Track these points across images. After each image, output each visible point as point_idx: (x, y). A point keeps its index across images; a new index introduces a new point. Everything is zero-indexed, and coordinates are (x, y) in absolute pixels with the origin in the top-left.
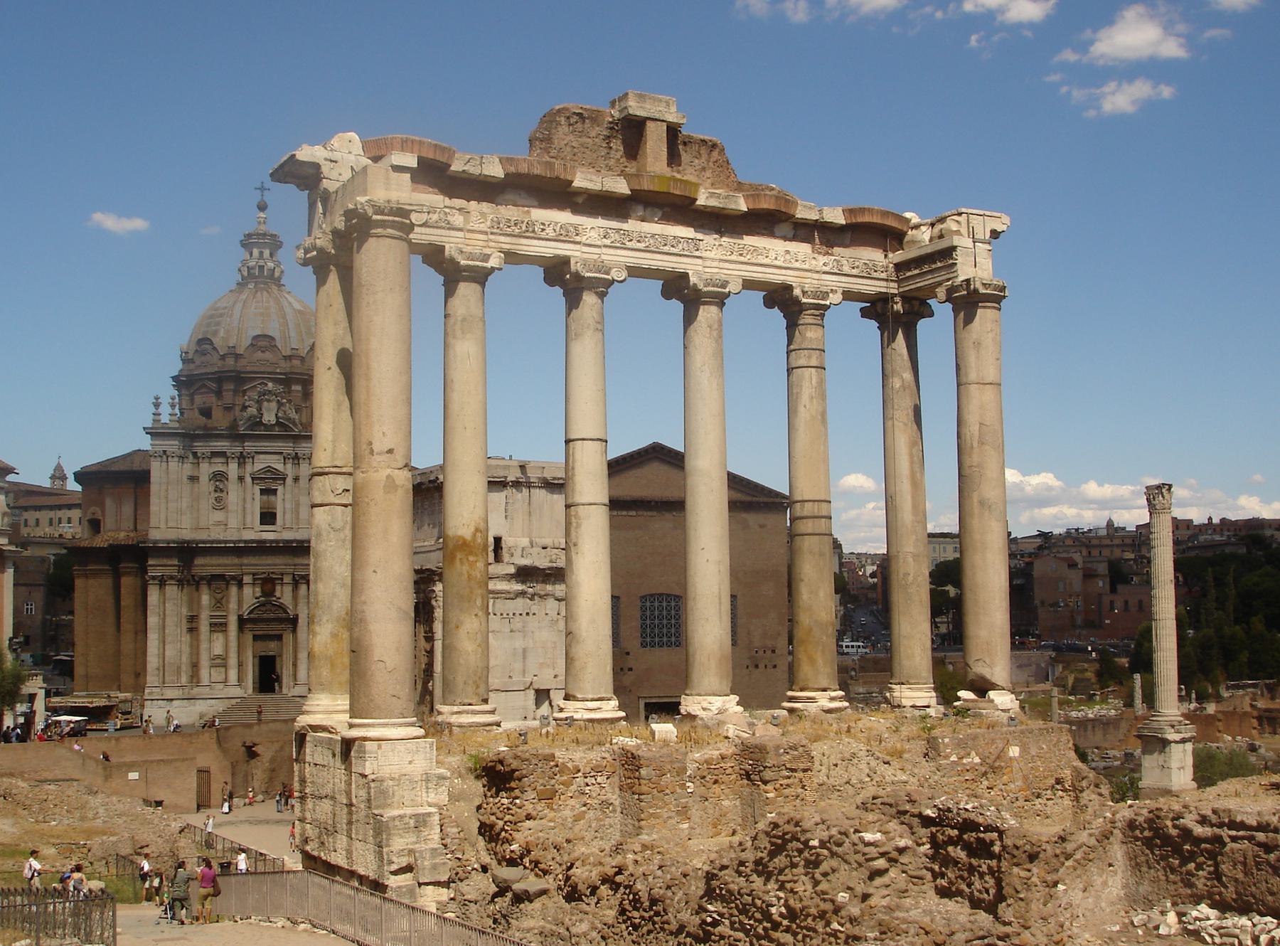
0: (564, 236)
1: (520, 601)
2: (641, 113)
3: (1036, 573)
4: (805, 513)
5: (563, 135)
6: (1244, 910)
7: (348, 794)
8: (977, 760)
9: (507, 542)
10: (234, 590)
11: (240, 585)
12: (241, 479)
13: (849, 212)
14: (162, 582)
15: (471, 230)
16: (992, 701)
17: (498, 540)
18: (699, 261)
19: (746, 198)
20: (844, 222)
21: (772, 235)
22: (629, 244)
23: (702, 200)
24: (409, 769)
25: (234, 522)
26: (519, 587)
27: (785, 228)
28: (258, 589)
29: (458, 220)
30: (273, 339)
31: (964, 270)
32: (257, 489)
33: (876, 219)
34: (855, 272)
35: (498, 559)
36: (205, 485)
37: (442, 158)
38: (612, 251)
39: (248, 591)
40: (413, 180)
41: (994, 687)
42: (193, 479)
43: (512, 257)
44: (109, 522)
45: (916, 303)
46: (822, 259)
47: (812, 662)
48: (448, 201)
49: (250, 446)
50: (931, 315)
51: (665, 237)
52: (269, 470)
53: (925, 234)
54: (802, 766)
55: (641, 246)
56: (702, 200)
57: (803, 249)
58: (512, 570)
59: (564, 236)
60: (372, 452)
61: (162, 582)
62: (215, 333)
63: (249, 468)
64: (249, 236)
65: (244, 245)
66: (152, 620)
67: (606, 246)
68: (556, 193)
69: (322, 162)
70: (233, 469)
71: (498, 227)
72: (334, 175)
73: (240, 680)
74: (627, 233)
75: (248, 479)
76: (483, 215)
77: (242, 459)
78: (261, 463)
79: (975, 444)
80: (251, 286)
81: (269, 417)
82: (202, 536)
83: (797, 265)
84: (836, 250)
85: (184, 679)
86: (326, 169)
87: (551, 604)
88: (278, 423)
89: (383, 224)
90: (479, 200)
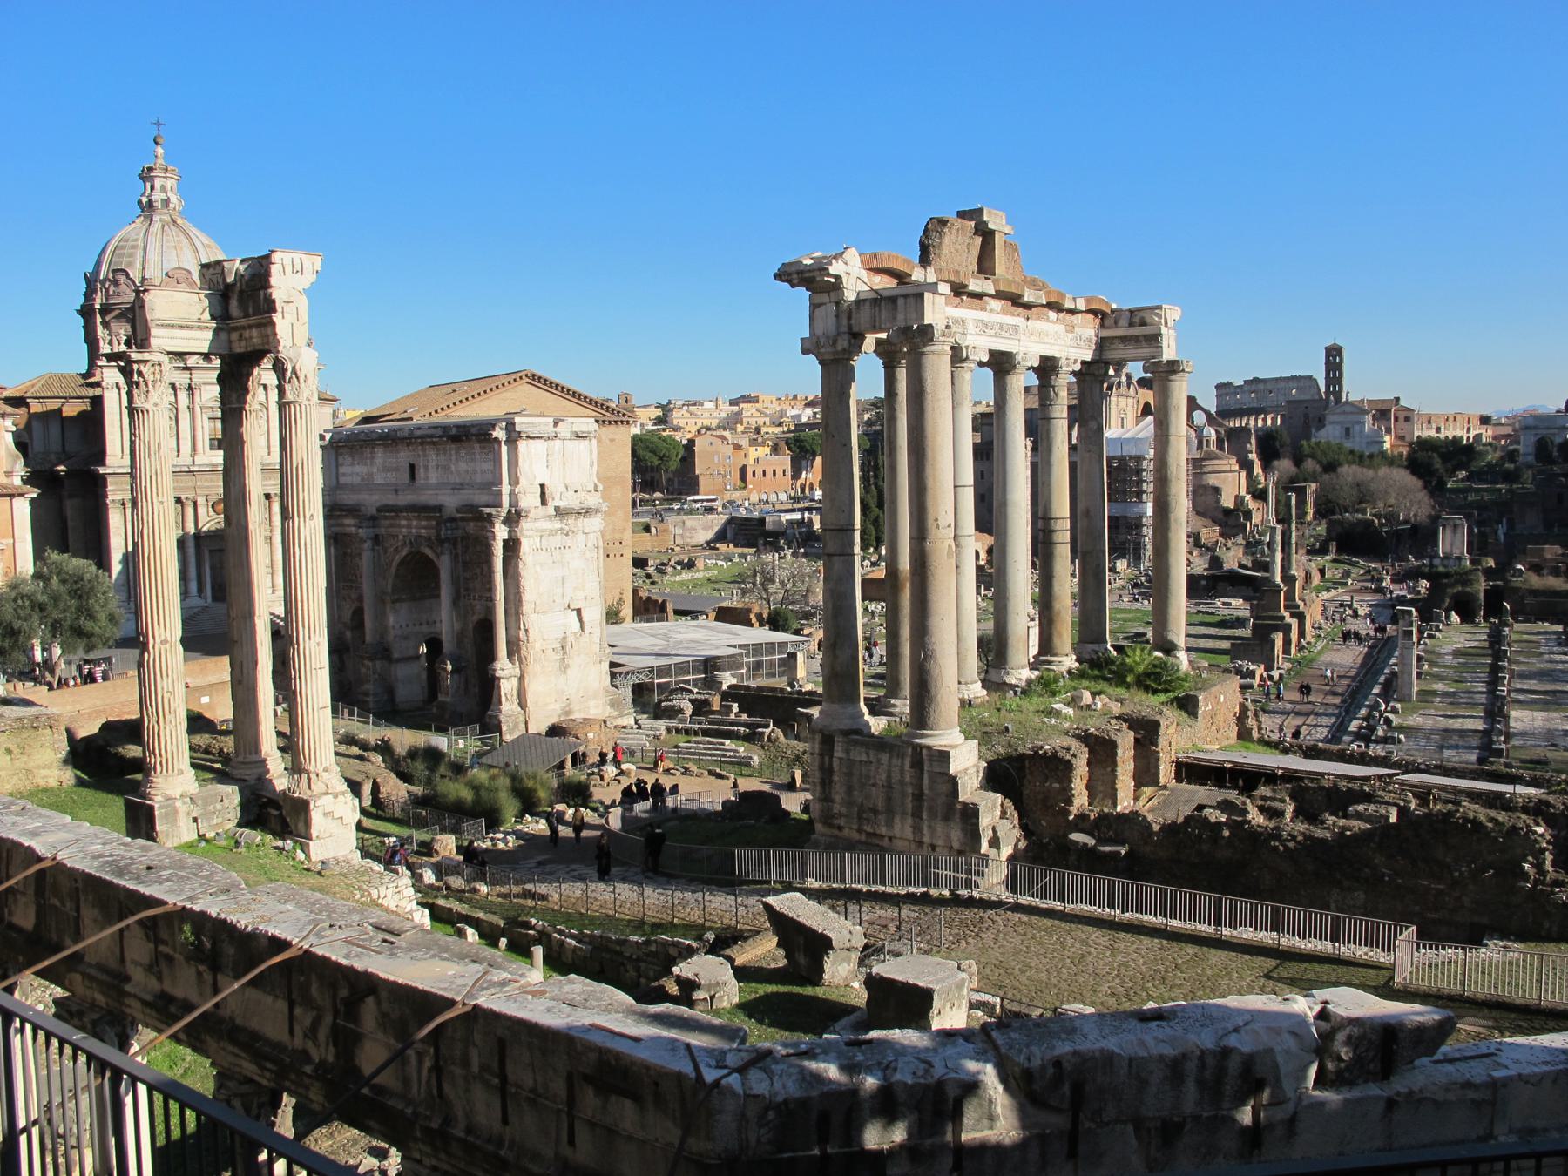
7: (919, 786)
12: (191, 409)
13: (1088, 301)
17: (542, 486)
26: (557, 525)
27: (1052, 315)
31: (1168, 354)
32: (205, 417)
35: (544, 502)
39: (202, 511)
46: (1070, 336)
47: (1060, 635)
51: (1001, 326)
57: (1061, 328)
62: (130, 264)
63: (197, 398)
65: (141, 177)
73: (200, 590)
87: (581, 538)
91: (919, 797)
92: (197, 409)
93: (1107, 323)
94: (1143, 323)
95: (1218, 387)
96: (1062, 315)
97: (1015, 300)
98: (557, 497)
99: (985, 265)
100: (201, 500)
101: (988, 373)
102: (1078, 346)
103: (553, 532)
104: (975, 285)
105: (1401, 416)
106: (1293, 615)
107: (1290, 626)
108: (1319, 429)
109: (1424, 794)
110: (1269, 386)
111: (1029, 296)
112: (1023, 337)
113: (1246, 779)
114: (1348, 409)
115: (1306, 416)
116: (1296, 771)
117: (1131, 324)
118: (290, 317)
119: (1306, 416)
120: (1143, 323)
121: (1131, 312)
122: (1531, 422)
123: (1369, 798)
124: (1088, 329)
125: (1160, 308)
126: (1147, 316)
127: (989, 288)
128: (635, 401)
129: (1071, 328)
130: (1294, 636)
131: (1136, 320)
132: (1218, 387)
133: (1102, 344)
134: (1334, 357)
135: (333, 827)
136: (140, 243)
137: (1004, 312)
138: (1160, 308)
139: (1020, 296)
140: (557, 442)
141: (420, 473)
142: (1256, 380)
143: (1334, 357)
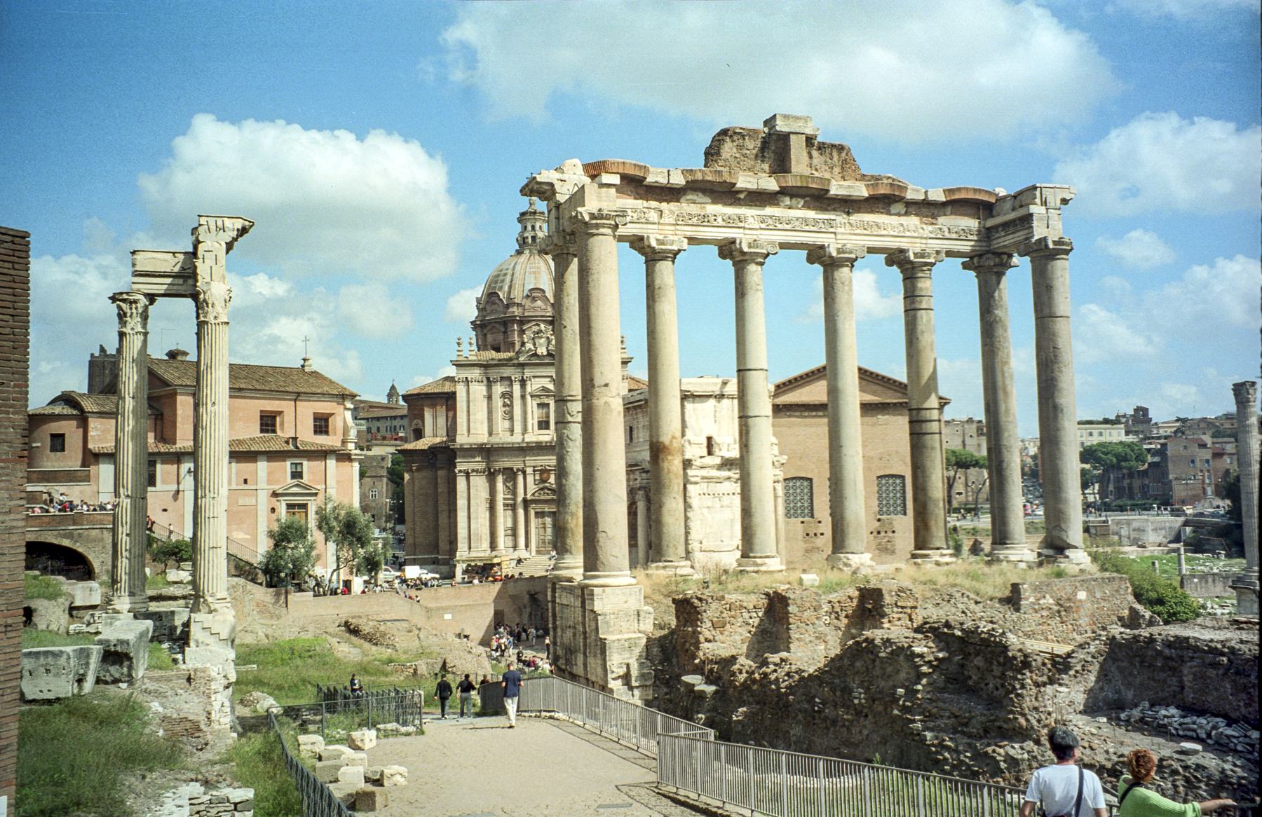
0: (728, 222)
1: (727, 484)
2: (787, 130)
3: (1169, 453)
5: (728, 149)
6: (1201, 713)
7: (584, 624)
8: (1051, 601)
9: (717, 439)
10: (520, 478)
11: (524, 473)
12: (523, 397)
14: (467, 475)
15: (662, 223)
16: (1067, 557)
17: (709, 439)
19: (867, 186)
21: (889, 213)
22: (780, 226)
23: (834, 191)
24: (626, 606)
25: (518, 428)
27: (899, 207)
28: (537, 477)
29: (653, 216)
30: (543, 291)
31: (1039, 232)
32: (535, 403)
33: (970, 196)
34: (954, 236)
35: (710, 453)
36: (498, 402)
37: (639, 173)
39: (530, 479)
40: (617, 191)
41: (1070, 547)
42: (490, 398)
43: (692, 240)
44: (428, 429)
45: (1005, 257)
48: (645, 204)
49: (528, 373)
52: (544, 389)
53: (1008, 205)
54: (909, 604)
55: (788, 227)
56: (834, 191)
57: (913, 221)
58: (718, 461)
59: (728, 222)
60: (593, 386)
61: (467, 475)
62: (501, 288)
63: (529, 389)
64: (523, 214)
66: (461, 502)
68: (726, 193)
69: (555, 182)
70: (517, 388)
71: (680, 220)
72: (564, 190)
73: (527, 546)
75: (528, 397)
76: (672, 212)
77: (523, 383)
78: (534, 386)
80: (527, 252)
81: (542, 351)
82: (495, 440)
83: (908, 234)
84: (941, 220)
85: (486, 544)
86: (557, 187)
88: (549, 355)
89: (597, 226)
90: (668, 202)
91: (585, 633)
92: (528, 397)
93: (994, 213)
97: (819, 199)
98: (724, 448)
99: (781, 165)
100: (529, 470)
101: (818, 268)
103: (719, 481)
104: (744, 181)
111: (837, 188)
112: (839, 230)
118: (210, 261)
121: (1015, 197)
124: (972, 223)
125: (1034, 188)
127: (772, 185)
128: (1155, 416)
133: (986, 234)
135: (211, 640)
136: (510, 272)
137: (807, 206)
138: (1034, 188)
139: (828, 191)
140: (725, 401)
141: (635, 432)
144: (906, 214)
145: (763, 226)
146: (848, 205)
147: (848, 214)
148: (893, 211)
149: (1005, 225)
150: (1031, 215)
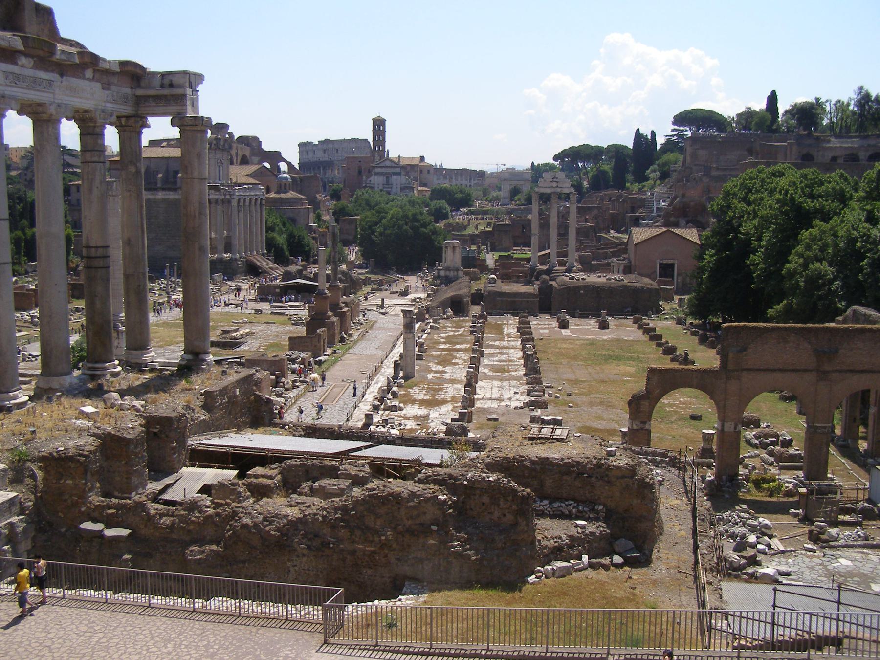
4: (98, 255)
18: (51, 95)
20: (119, 70)
21: (84, 78)
27: (89, 73)
38: (9, 89)
46: (107, 92)
50: (149, 127)
51: (35, 80)
53: (157, 82)
57: (99, 85)
67: (7, 85)
74: (17, 77)
79: (197, 214)
93: (143, 84)
94: (171, 85)
95: (301, 145)
96: (97, 75)
102: (114, 101)
105: (425, 172)
106: (335, 315)
107: (333, 322)
108: (368, 177)
109: (380, 469)
110: (336, 146)
113: (243, 460)
114: (388, 163)
115: (360, 167)
116: (283, 452)
117: (162, 86)
119: (360, 167)
120: (171, 85)
121: (164, 75)
122: (507, 176)
123: (333, 473)
126: (176, 80)
127: (19, 45)
129: (106, 86)
130: (337, 331)
131: (166, 81)
132: (301, 145)
133: (139, 101)
134: (379, 125)
137: (35, 67)
142: (327, 141)
143: (379, 125)
144: (93, 79)
145: (8, 82)
146: (64, 69)
147: (62, 75)
148: (87, 76)
149: (157, 98)
150: (184, 96)
